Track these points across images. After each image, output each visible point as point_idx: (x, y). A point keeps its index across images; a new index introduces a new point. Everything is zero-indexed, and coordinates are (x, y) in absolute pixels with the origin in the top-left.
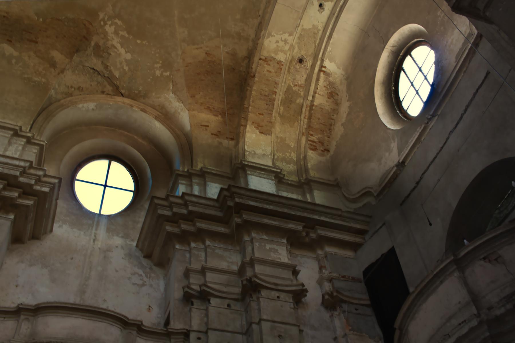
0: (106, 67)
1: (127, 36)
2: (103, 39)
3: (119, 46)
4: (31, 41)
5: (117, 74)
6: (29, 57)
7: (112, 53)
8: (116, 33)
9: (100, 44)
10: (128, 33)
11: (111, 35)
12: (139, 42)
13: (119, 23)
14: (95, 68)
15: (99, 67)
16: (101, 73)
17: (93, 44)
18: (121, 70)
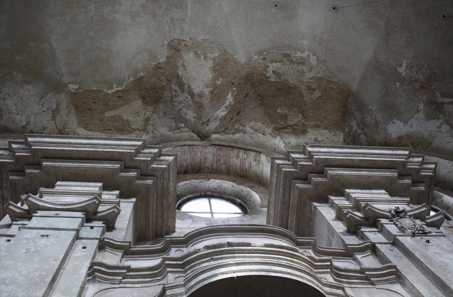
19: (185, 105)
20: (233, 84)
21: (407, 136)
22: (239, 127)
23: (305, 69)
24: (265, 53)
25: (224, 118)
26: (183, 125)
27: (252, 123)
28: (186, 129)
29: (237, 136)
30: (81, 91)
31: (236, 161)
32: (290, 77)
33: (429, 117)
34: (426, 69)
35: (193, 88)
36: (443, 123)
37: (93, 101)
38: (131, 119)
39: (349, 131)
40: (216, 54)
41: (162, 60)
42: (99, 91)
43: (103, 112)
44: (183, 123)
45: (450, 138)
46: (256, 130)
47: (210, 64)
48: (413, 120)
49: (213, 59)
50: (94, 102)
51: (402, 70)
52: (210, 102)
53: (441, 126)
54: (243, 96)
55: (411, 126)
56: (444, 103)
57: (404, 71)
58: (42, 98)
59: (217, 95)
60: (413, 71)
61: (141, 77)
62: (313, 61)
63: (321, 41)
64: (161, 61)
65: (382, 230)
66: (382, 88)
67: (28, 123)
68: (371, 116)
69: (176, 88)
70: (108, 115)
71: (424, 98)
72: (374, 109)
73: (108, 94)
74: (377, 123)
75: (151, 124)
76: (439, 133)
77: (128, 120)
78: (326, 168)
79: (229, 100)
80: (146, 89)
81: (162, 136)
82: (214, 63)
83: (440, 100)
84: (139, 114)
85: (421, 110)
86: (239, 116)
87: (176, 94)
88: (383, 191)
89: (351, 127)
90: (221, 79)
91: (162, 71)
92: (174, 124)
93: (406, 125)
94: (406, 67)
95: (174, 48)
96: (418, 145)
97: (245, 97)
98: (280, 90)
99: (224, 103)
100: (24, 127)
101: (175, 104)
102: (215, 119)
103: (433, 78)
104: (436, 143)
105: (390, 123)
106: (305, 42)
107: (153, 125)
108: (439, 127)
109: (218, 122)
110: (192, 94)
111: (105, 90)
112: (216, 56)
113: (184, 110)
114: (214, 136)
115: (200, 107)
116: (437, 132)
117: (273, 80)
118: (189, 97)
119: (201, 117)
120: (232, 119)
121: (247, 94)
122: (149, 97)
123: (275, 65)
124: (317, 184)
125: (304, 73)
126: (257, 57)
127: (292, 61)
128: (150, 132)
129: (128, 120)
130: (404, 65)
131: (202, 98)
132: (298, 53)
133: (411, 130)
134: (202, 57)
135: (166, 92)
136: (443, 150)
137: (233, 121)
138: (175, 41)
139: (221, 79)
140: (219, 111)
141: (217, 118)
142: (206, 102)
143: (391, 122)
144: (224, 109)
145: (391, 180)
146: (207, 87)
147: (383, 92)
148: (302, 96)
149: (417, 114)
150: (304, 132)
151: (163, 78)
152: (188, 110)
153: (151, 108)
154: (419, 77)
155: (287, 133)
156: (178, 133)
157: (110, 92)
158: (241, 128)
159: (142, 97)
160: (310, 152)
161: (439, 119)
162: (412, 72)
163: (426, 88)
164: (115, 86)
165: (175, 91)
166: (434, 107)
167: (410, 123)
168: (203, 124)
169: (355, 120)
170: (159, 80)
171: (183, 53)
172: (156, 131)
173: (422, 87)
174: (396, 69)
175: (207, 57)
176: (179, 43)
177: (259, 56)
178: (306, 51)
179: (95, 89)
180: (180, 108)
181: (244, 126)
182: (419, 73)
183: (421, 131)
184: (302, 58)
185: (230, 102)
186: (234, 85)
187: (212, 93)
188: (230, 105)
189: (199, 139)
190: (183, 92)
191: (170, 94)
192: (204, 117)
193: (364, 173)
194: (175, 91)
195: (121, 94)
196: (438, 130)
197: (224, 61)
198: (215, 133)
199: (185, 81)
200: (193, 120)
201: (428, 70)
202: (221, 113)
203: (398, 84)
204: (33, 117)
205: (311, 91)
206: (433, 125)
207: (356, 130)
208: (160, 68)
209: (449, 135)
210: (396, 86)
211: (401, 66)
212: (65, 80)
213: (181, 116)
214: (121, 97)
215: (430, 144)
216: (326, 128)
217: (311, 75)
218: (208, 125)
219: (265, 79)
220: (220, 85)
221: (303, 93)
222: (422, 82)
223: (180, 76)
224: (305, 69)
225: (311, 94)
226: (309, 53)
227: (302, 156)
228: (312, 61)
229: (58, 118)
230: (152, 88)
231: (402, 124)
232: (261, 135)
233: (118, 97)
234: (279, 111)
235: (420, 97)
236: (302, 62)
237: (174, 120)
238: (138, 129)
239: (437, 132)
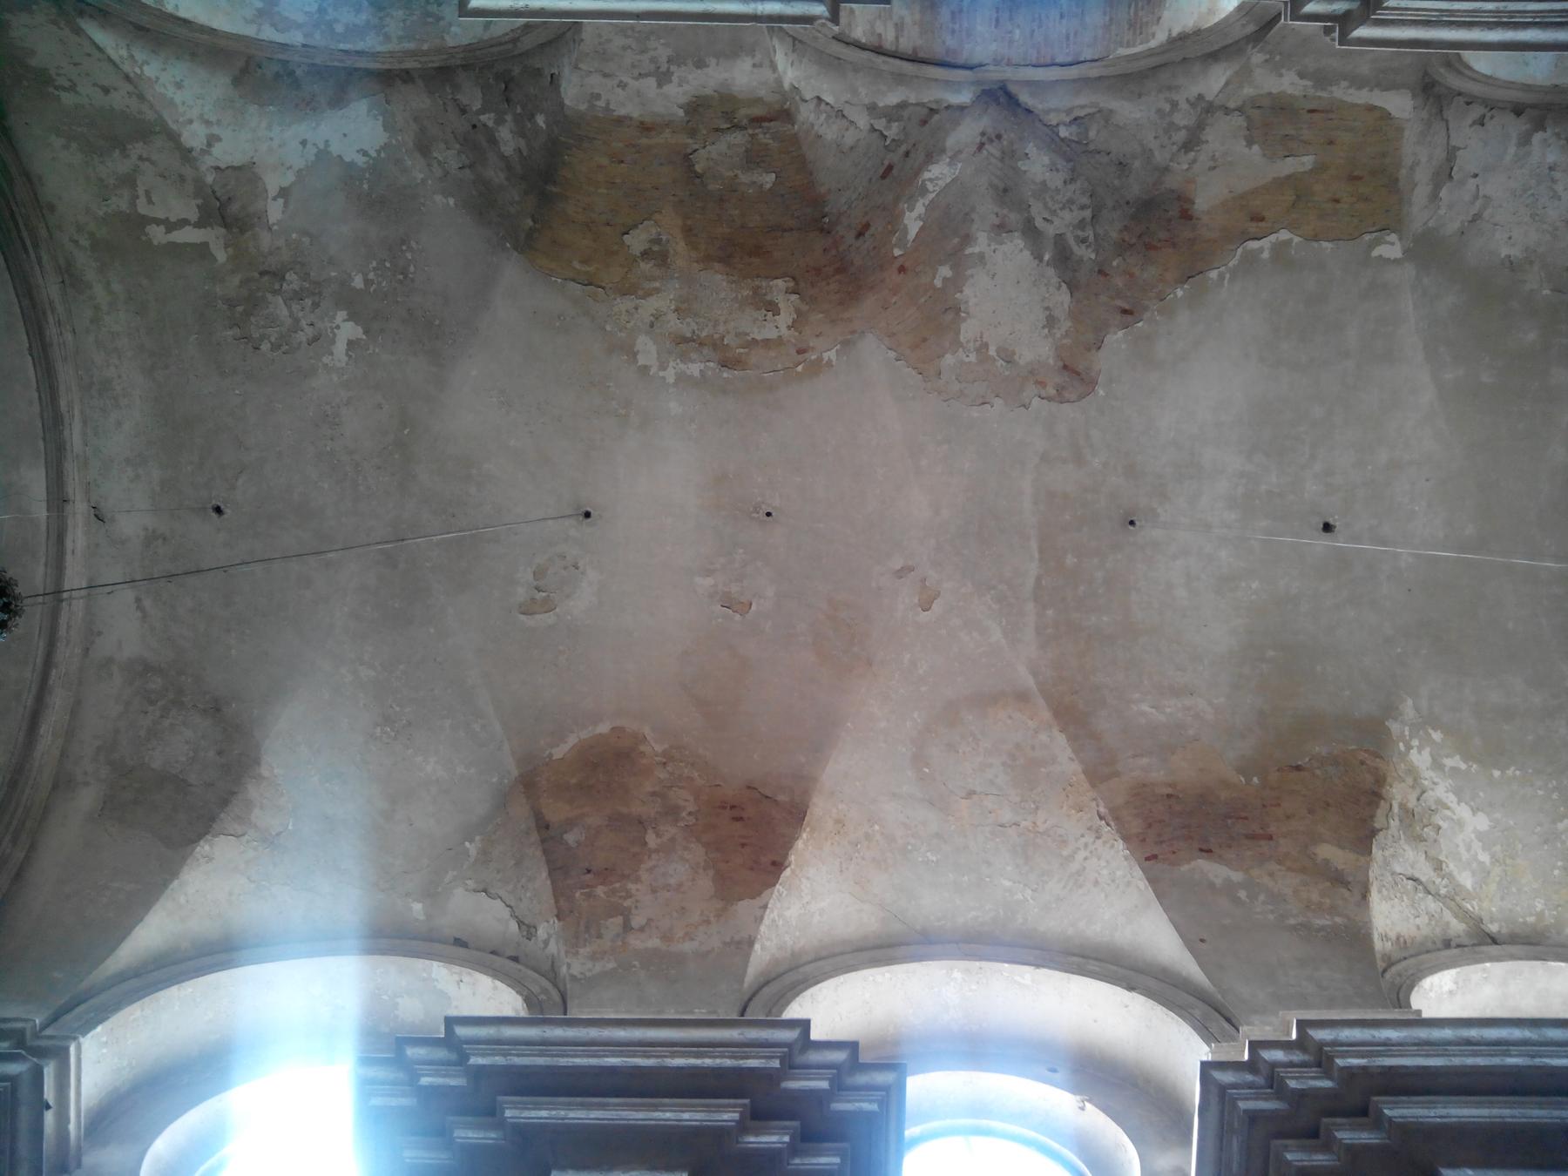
0: (1438, 866)
1: (1463, 766)
2: (1413, 787)
3: (1451, 799)
4: (1252, 837)
5: (1467, 880)
6: (1271, 875)
7: (1441, 823)
8: (1437, 765)
9: (1410, 805)
10: (1466, 759)
11: (1428, 775)
12: (1497, 773)
13: (1437, 736)
14: (1417, 875)
15: (1425, 872)
16: (1432, 888)
17: (1396, 809)
18: (1474, 865)
19: (1052, 198)
20: (902, 269)
21: (314, 109)
22: (888, 128)
23: (673, 323)
24: (800, 368)
25: (930, 158)
26: (1063, 132)
27: (849, 138)
28: (1053, 119)
29: (892, 99)
30: (1367, 237)
31: (904, 12)
32: (722, 295)
33: (246, 173)
34: (263, 337)
35: (1027, 253)
36: (204, 152)
37: (1338, 206)
38: (1240, 147)
39: (532, 117)
40: (949, 359)
41: (1116, 338)
42: (1316, 238)
43: (1319, 168)
44: (1062, 140)
45: (178, 98)
46: (841, 114)
47: (968, 330)
48: (299, 163)
49: (961, 345)
50: (1337, 201)
51: (348, 330)
52: (973, 209)
53: (209, 145)
54: (872, 230)
55: (304, 143)
56: (198, 225)
57: (338, 327)
58: (1476, 218)
59: (950, 231)
61: (1184, 282)
62: (647, 350)
63: (623, 412)
64: (1120, 334)
66: (412, 269)
67: (1525, 140)
68: (447, 173)
69: (1081, 252)
70: (1305, 159)
71: (266, 240)
72: (438, 198)
73: (1292, 227)
74: (424, 148)
75: (1179, 129)
76: (213, 119)
77: (1250, 143)
79: (915, 214)
80: (1174, 245)
81: (1140, 96)
82: (958, 333)
83: (212, 236)
84: (1212, 164)
85: (274, 199)
86: (886, 163)
87: (1083, 229)
89: (520, 132)
90: (938, 283)
91: (1119, 303)
92: (1092, 134)
93: (322, 146)
94: (333, 342)
95: (1078, 374)
96: (277, 76)
97: (867, 226)
98: (757, 251)
99: (931, 207)
100: (1540, 126)
101: (1085, 200)
102: (960, 152)
103: (240, 309)
105: (378, 152)
106: (674, 407)
107: (1172, 127)
108: (212, 140)
109: (950, 142)
110: (1031, 232)
111: (1297, 239)
112: (948, 356)
113: (1056, 180)
114: (964, 97)
115: (1005, 190)
116: (219, 122)
117: (779, 282)
118: (1039, 223)
119: (1002, 160)
120: (907, 154)
121: (860, 234)
122: (1170, 220)
123: (770, 333)
125: (676, 310)
126: (826, 356)
127: (717, 345)
128: (1184, 105)
129: (1250, 143)
130: (340, 347)
131: (997, 221)
132: (696, 374)
133: (302, 129)
134: (992, 352)
135: (1114, 235)
136: (193, 55)
137: (903, 148)
138: (1073, 397)
139: (938, 283)
140: (949, 180)
141: (954, 158)
142: (986, 209)
143: (374, 154)
144: (930, 186)
146: (981, 256)
147: (409, 256)
148: (688, 232)
149: (285, 184)
150: (696, 107)
151: (1119, 282)
152: (1044, 183)
153: (1172, 182)
154: (289, 308)
155: (758, 101)
156: (1083, 107)
157: (1284, 235)
158: (880, 124)
159: (1190, 218)
161: (217, 168)
163: (262, 274)
164: (1266, 255)
165: (1084, 241)
166: (234, 208)
167: (311, 151)
168: (999, 137)
169: (503, 157)
170: (1132, 275)
171: (1051, 361)
172: (1159, 111)
173: (279, 275)
174: (366, 332)
175: (978, 350)
176: (1060, 389)
177: (820, 359)
178: (671, 380)
179: (1325, 244)
180: (1072, 187)
181: (873, 129)
182: (289, 321)
183: (269, 128)
184: (684, 358)
185: (911, 209)
186: (897, 264)
187: (967, 239)
188: (912, 200)
189: (1013, 88)
190: (1059, 238)
191: (1101, 232)
192: (993, 161)
194: (1084, 241)
195: (1253, 228)
196: (216, 130)
197: (925, 340)
198: (962, 108)
199: (1051, 272)
200: (1031, 148)
201: (256, 335)
202: (939, 174)
203: (358, 282)
204: (1508, 158)
205: (656, 248)
206: (231, 149)
207: (500, 121)
208: (1125, 312)
209: (181, 109)
210: (365, 275)
211: (351, 344)
212: (1409, 270)
213: (1069, 160)
214: (1252, 219)
215: (237, 82)
216: (620, 121)
217: (652, 305)
218: (983, 134)
219: (802, 285)
220: (941, 263)
221: (682, 244)
222: (275, 292)
223: (1064, 286)
224: (673, 323)
225: (658, 241)
226: (661, 374)
228: (653, 348)
229: (1440, 154)
230: (1155, 248)
231: (335, 149)
232: (828, 98)
233: (1262, 219)
234: (769, 179)
235: (281, 242)
236: (684, 344)
237: (1092, 147)
238: (1227, 111)
239: (219, 122)
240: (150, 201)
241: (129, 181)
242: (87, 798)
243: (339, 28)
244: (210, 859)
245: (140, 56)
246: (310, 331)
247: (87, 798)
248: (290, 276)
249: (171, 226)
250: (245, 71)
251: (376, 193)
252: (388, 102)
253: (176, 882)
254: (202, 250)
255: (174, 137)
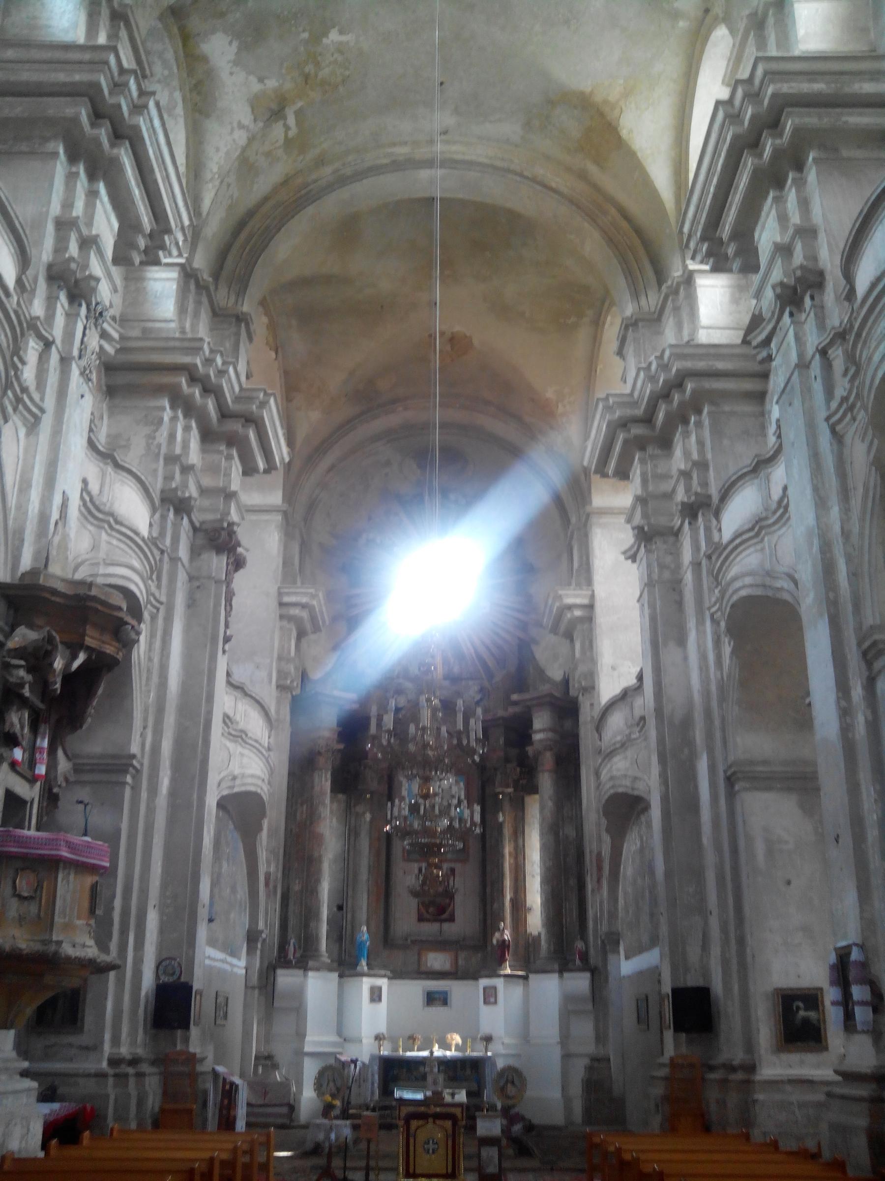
33: (255, 103)
36: (248, 130)
51: (334, 36)
55: (231, 74)
60: (336, 55)
65: (71, 317)
71: (288, 85)
74: (222, 15)
78: (127, 143)
88: (116, 225)
93: (231, 65)
96: (199, 93)
104: (211, 126)
108: (241, 126)
124: (97, 141)
130: (344, 38)
133: (224, 75)
136: (201, 143)
145: (137, 227)
160: (146, 106)
161: (255, 120)
162: (333, 55)
166: (274, 106)
173: (307, 77)
174: (334, 27)
193: (137, 192)
196: (235, 125)
203: (306, 35)
206: (242, 114)
215: (208, 116)
222: (316, 76)
227: (135, 94)
231: (231, 57)
239: (231, 123)
240: (277, 141)
241: (268, 154)
242: (592, 169)
243: (166, 72)
244: (631, 131)
245: (208, 176)
246: (336, 55)
247: (592, 169)
248: (307, 70)
249: (287, 128)
250: (200, 112)
251: (252, 34)
252: (198, 34)
253: (639, 155)
254: (298, 113)
255: (244, 149)
